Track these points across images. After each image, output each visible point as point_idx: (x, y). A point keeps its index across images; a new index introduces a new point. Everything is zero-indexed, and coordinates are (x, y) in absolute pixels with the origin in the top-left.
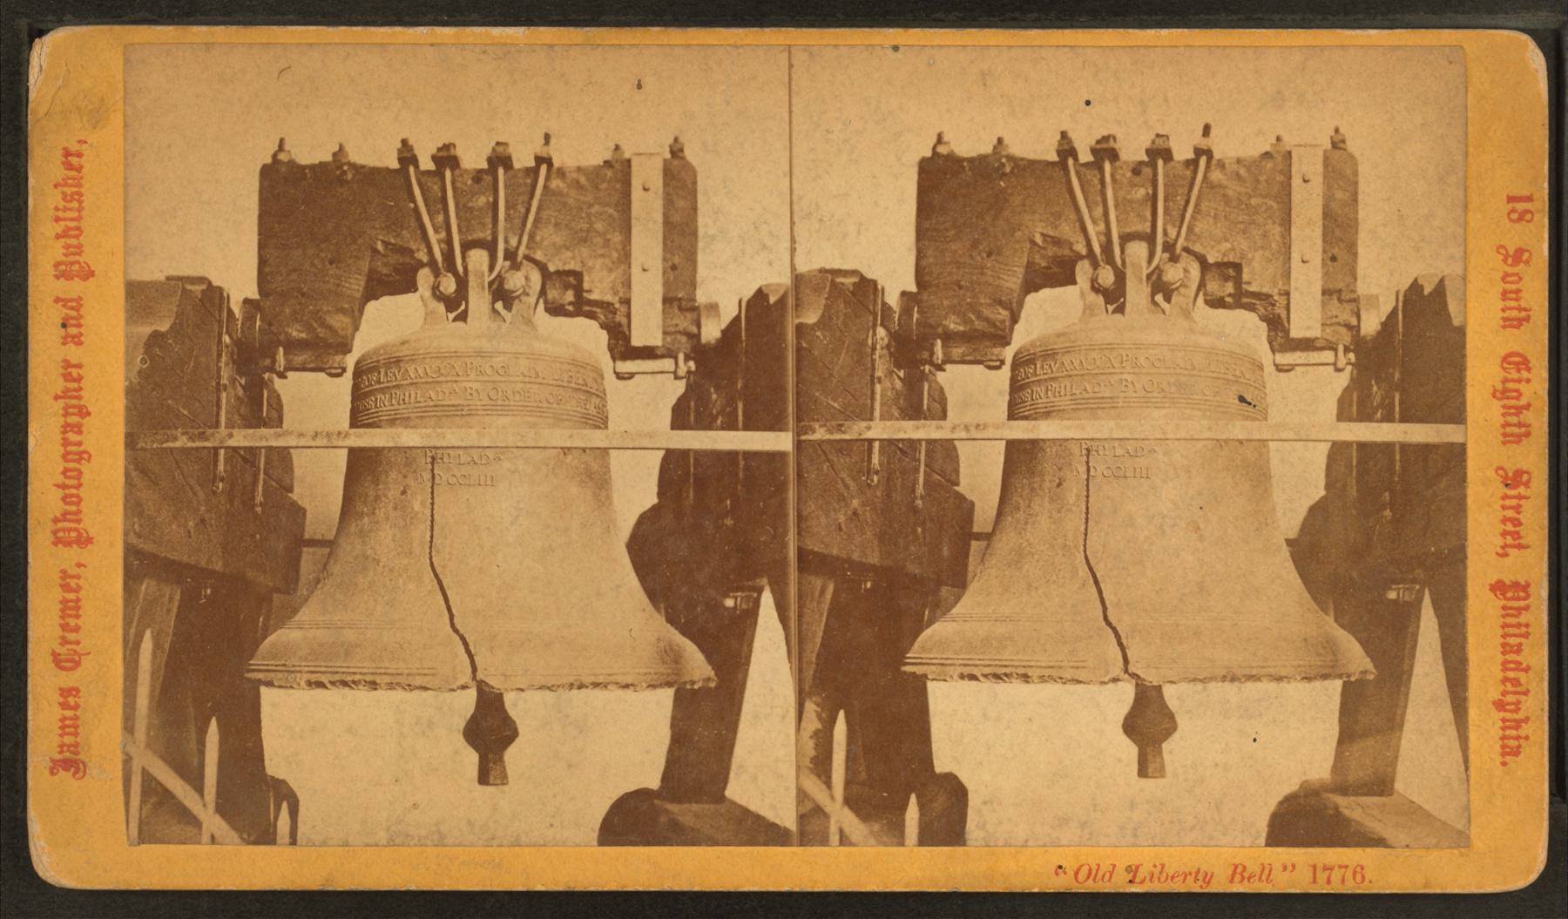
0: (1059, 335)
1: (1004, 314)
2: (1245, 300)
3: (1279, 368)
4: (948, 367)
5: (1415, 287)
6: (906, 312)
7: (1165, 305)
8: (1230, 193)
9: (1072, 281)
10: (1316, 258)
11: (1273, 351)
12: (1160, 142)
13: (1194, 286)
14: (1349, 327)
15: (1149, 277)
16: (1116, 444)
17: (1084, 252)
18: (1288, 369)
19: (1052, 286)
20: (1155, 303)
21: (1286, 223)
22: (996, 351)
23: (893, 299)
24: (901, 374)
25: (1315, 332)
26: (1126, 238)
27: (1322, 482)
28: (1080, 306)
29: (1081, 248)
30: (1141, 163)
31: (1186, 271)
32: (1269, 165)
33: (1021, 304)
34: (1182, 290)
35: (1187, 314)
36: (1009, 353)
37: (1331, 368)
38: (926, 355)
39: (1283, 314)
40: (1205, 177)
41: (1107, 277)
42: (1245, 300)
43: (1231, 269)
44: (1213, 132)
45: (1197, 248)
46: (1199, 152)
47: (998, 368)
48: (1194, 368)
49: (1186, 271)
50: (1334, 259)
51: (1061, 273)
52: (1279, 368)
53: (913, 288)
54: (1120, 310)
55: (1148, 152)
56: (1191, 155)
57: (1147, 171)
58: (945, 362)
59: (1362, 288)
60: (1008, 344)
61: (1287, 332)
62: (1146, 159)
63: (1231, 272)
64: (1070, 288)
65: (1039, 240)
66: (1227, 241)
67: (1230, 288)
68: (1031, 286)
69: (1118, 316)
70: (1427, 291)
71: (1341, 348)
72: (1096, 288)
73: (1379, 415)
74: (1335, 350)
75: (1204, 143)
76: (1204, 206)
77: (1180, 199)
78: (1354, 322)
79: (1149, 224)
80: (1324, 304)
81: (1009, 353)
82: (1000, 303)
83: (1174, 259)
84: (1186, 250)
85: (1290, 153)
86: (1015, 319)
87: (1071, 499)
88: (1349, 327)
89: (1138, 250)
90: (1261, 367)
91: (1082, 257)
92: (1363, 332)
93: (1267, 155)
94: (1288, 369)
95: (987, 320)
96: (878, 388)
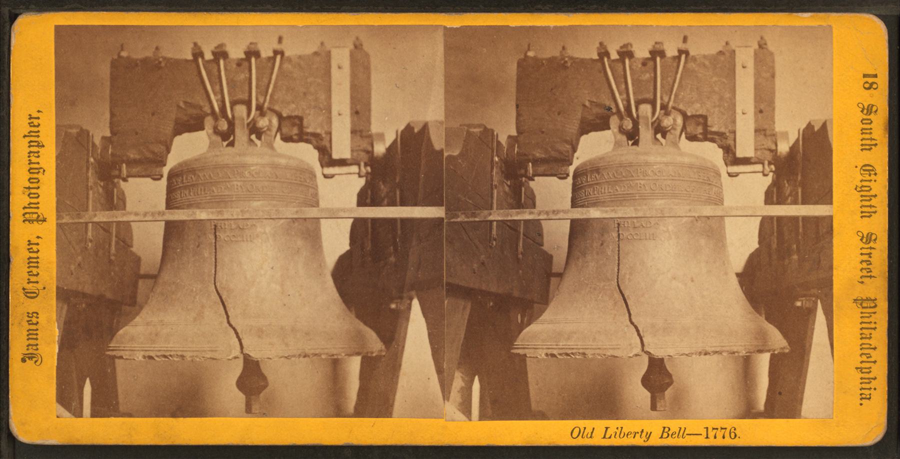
0: (196, 160)
1: (163, 148)
2: (305, 137)
3: (326, 176)
4: (130, 179)
5: (409, 128)
6: (105, 148)
7: (258, 142)
8: (295, 75)
9: (200, 127)
10: (347, 111)
11: (322, 166)
12: (253, 46)
13: (274, 129)
14: (368, 152)
15: (248, 124)
16: (232, 222)
17: (209, 111)
18: (332, 176)
19: (190, 131)
20: (251, 140)
21: (329, 91)
22: (158, 169)
23: (97, 141)
24: (102, 184)
25: (347, 155)
26: (233, 104)
27: (347, 241)
28: (207, 141)
29: (207, 109)
30: (242, 59)
31: (270, 121)
32: (318, 59)
33: (172, 141)
34: (268, 132)
35: (271, 147)
36: (166, 171)
37: (357, 176)
38: (117, 173)
39: (328, 145)
40: (280, 68)
41: (224, 126)
42: (305, 137)
43: (297, 121)
44: (284, 41)
45: (277, 108)
46: (276, 52)
47: (159, 179)
48: (277, 177)
49: (270, 121)
50: (357, 113)
51: (197, 126)
52: (326, 176)
53: (108, 134)
54: (232, 144)
55: (246, 53)
56: (271, 54)
57: (246, 64)
58: (128, 176)
59: (375, 129)
60: (165, 165)
61: (331, 156)
62: (243, 56)
63: (297, 121)
64: (200, 132)
65: (182, 104)
66: (293, 102)
67: (295, 131)
68: (178, 132)
69: (230, 148)
70: (416, 130)
71: (362, 164)
72: (216, 131)
73: (385, 202)
74: (359, 165)
75: (278, 47)
76: (280, 83)
77: (266, 80)
78: (370, 149)
79: (247, 95)
80: (352, 138)
81: (166, 171)
82: (161, 142)
83: (262, 114)
84: (270, 109)
85: (330, 52)
86: (168, 150)
87: (206, 255)
88: (368, 152)
89: (241, 110)
90: (315, 176)
91: (208, 115)
92: (375, 155)
93: (316, 53)
94: (332, 176)
95: (153, 153)
96: (91, 192)
